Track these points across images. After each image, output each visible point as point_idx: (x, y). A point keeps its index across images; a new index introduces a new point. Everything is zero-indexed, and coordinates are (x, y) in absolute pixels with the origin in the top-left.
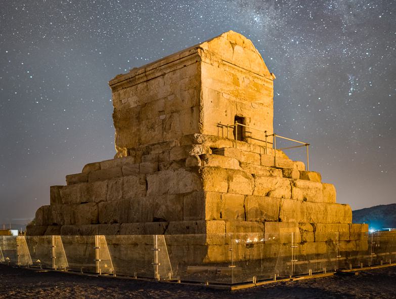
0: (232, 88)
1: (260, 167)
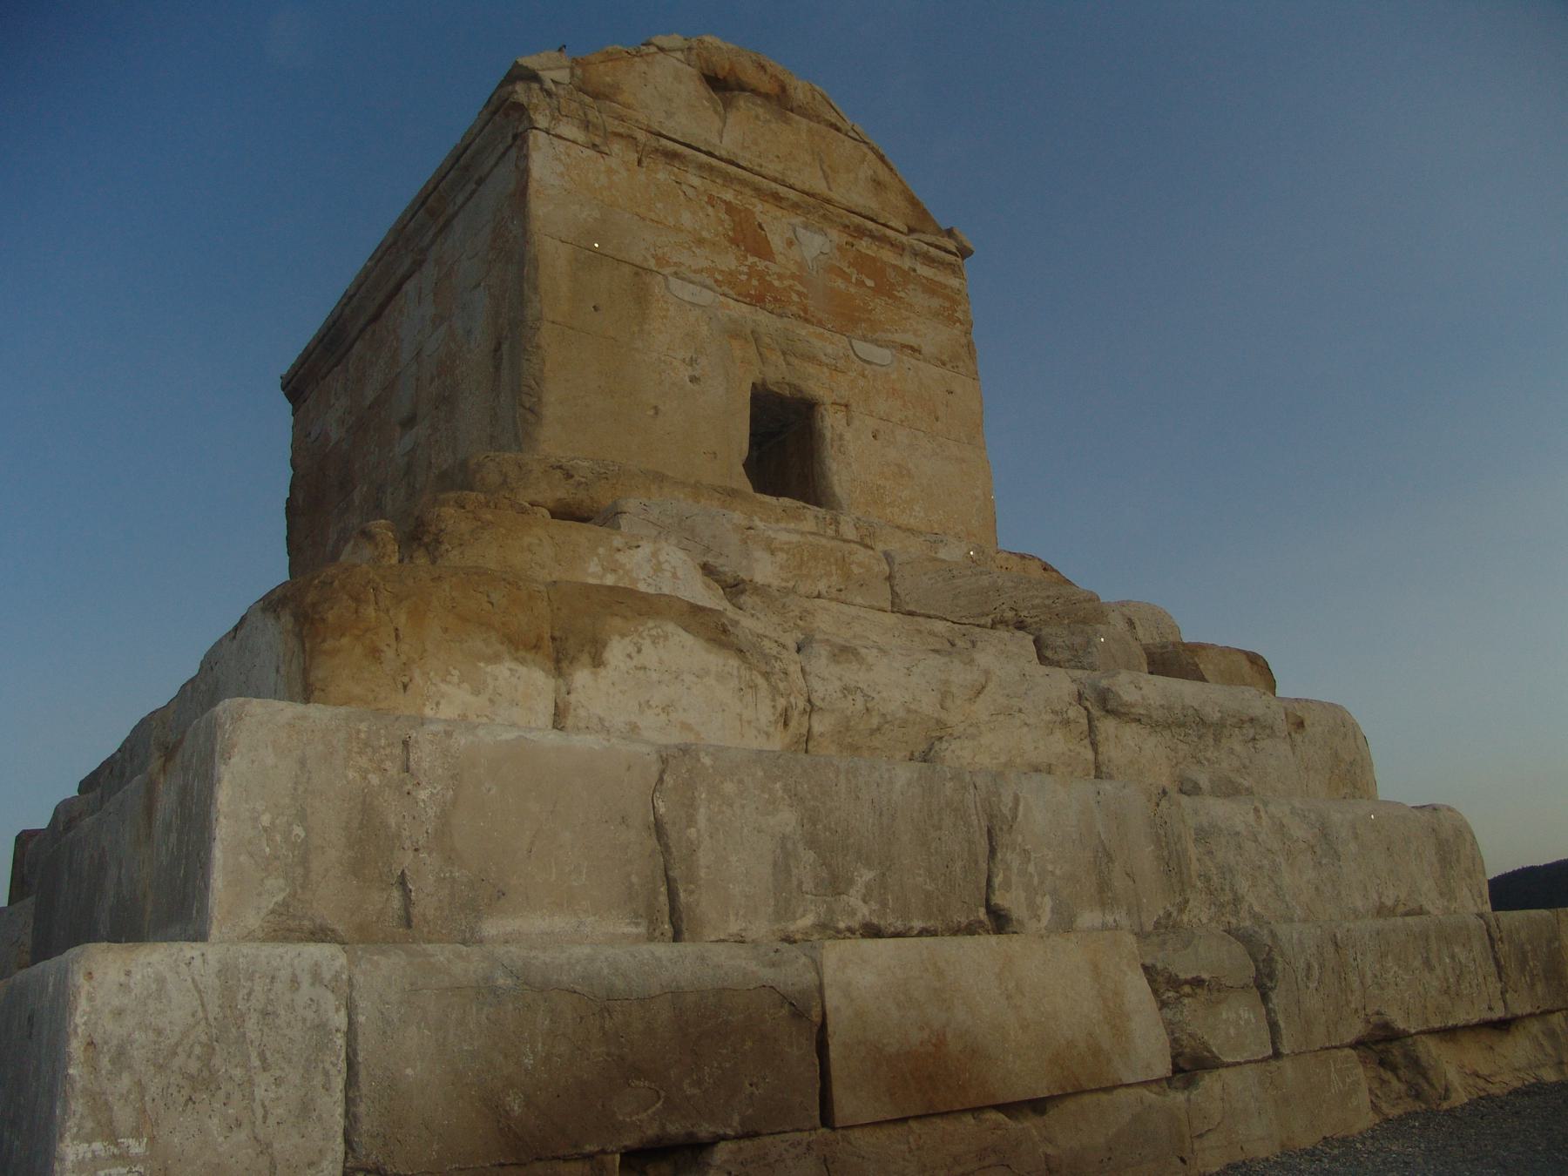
1: (890, 619)
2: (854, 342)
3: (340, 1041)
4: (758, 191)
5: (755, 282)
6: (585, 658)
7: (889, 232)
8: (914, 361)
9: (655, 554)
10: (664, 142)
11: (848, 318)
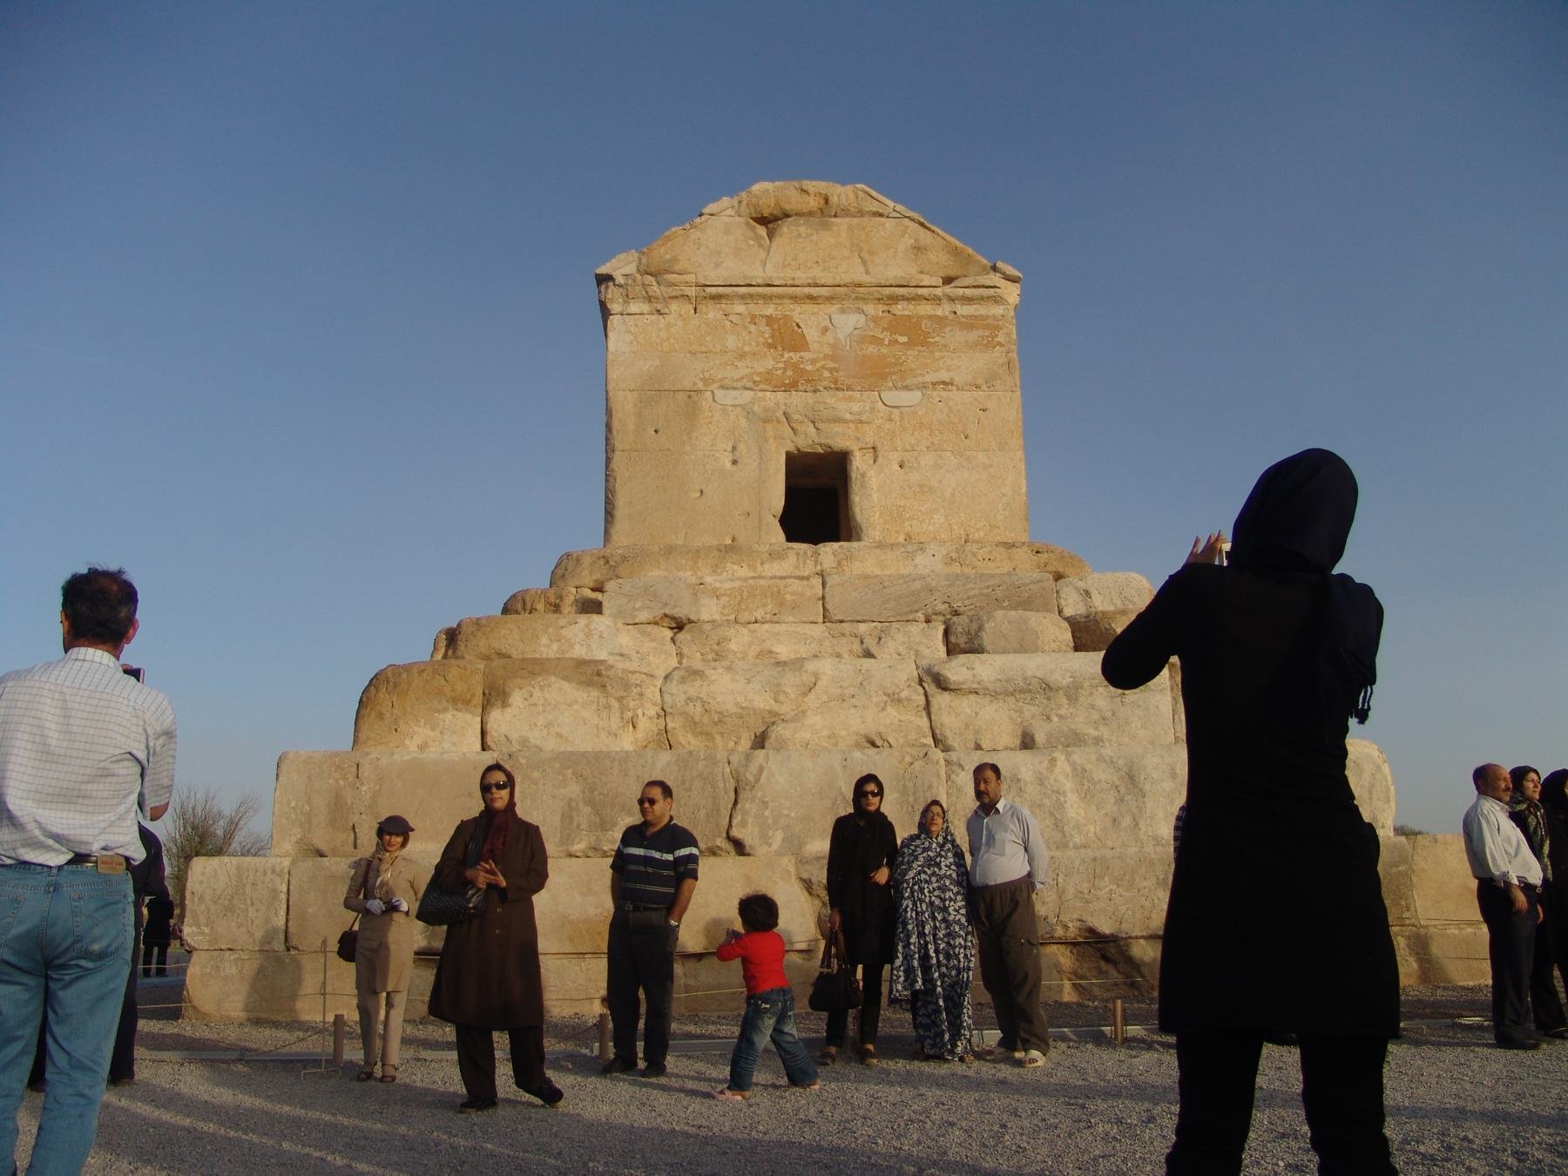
0: (769, 363)
1: (819, 630)
2: (885, 395)
3: (283, 897)
4: (794, 298)
5: (789, 373)
6: (499, 703)
7: (920, 291)
8: (944, 394)
9: (587, 626)
10: (709, 290)
11: (877, 375)
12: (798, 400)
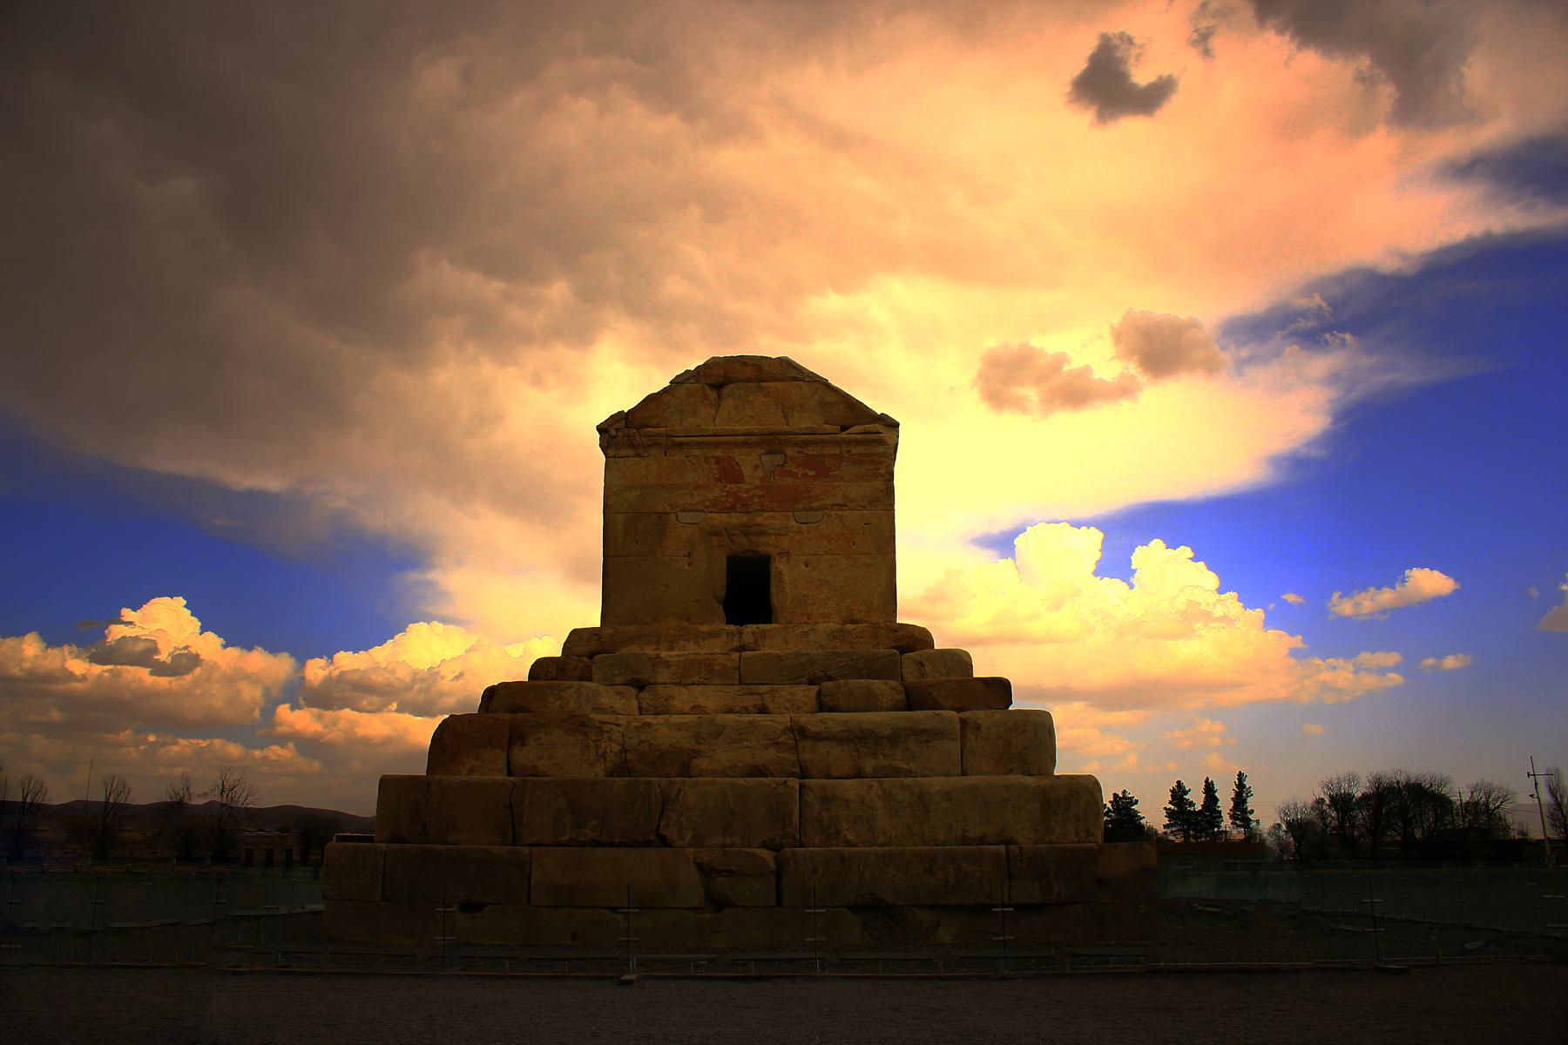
12: (736, 519)
